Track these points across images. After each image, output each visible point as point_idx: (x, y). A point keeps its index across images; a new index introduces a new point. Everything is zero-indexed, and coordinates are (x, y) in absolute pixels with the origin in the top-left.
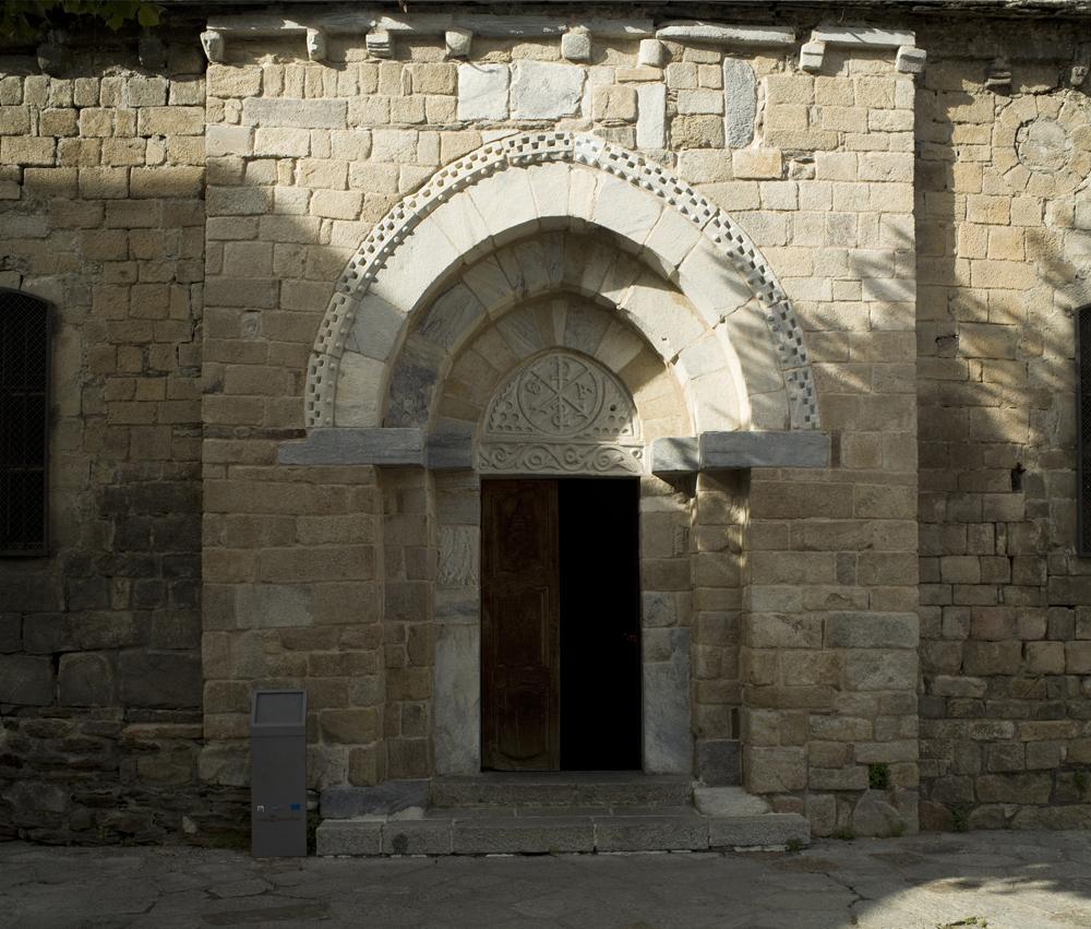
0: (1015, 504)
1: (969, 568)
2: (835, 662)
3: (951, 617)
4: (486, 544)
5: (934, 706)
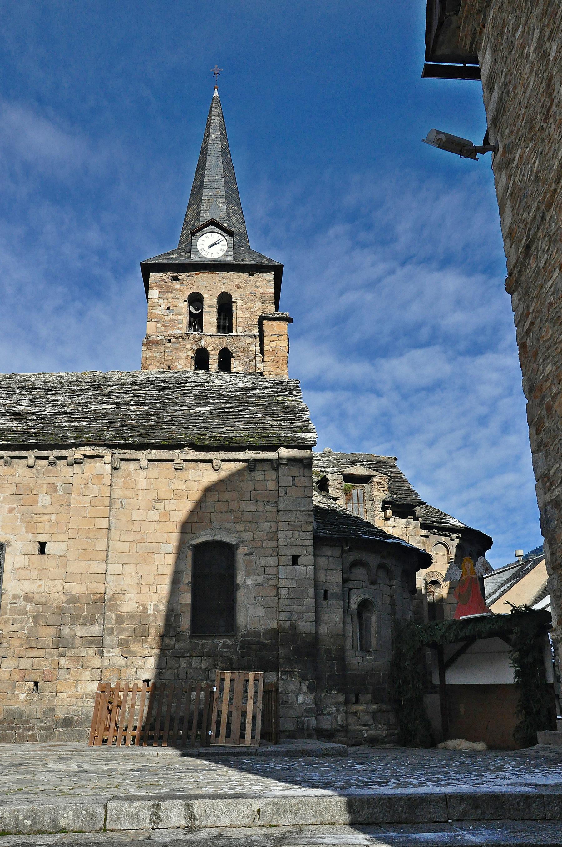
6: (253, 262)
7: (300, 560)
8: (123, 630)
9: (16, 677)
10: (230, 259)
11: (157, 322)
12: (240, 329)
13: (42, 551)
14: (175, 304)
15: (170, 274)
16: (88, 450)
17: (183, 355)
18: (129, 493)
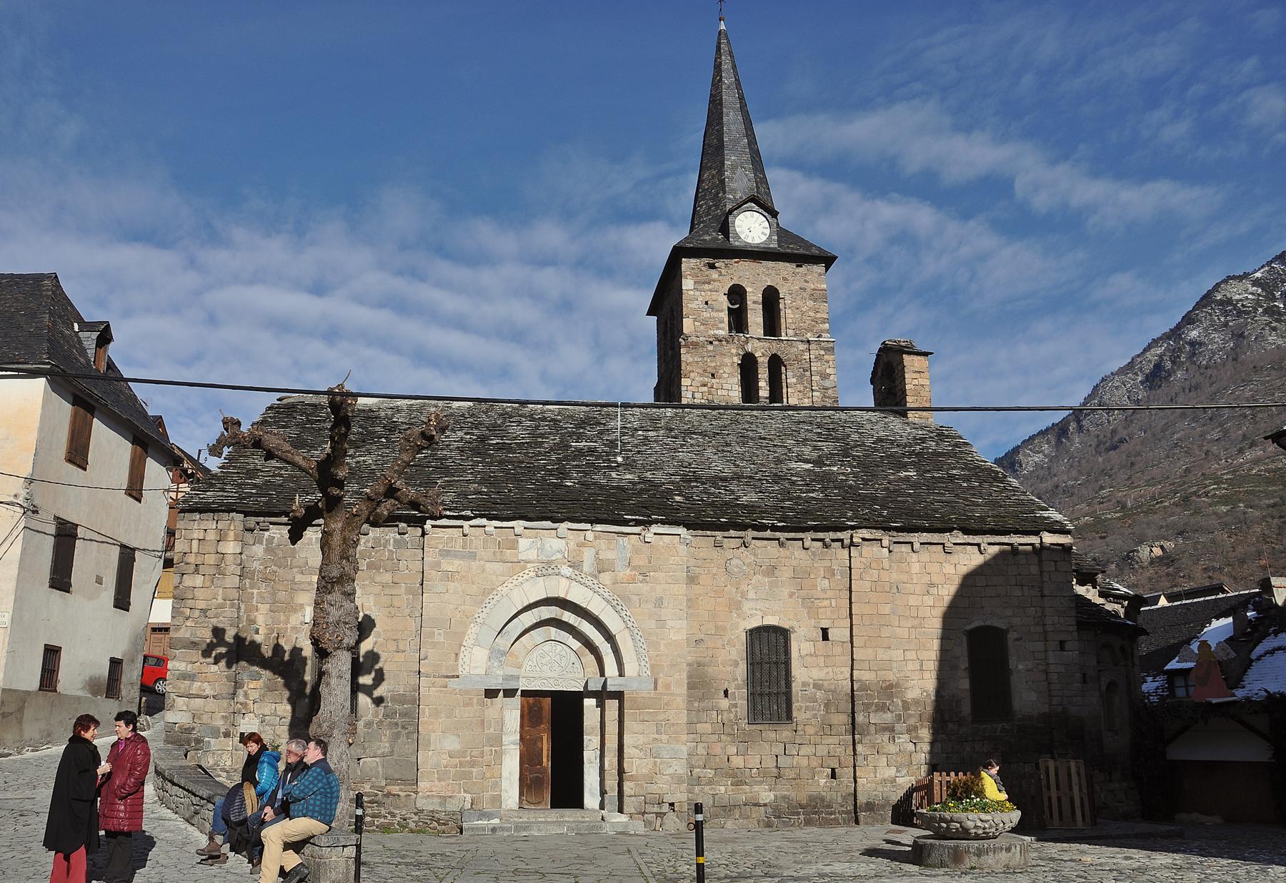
0: (725, 703)
1: (707, 728)
2: (655, 763)
3: (700, 746)
4: (522, 716)
5: (695, 781)
6: (802, 251)
7: (1067, 646)
8: (910, 716)
9: (814, 764)
10: (774, 245)
11: (695, 320)
12: (791, 332)
13: (825, 637)
14: (714, 297)
15: (706, 260)
16: (865, 533)
17: (727, 360)
18: (904, 577)
